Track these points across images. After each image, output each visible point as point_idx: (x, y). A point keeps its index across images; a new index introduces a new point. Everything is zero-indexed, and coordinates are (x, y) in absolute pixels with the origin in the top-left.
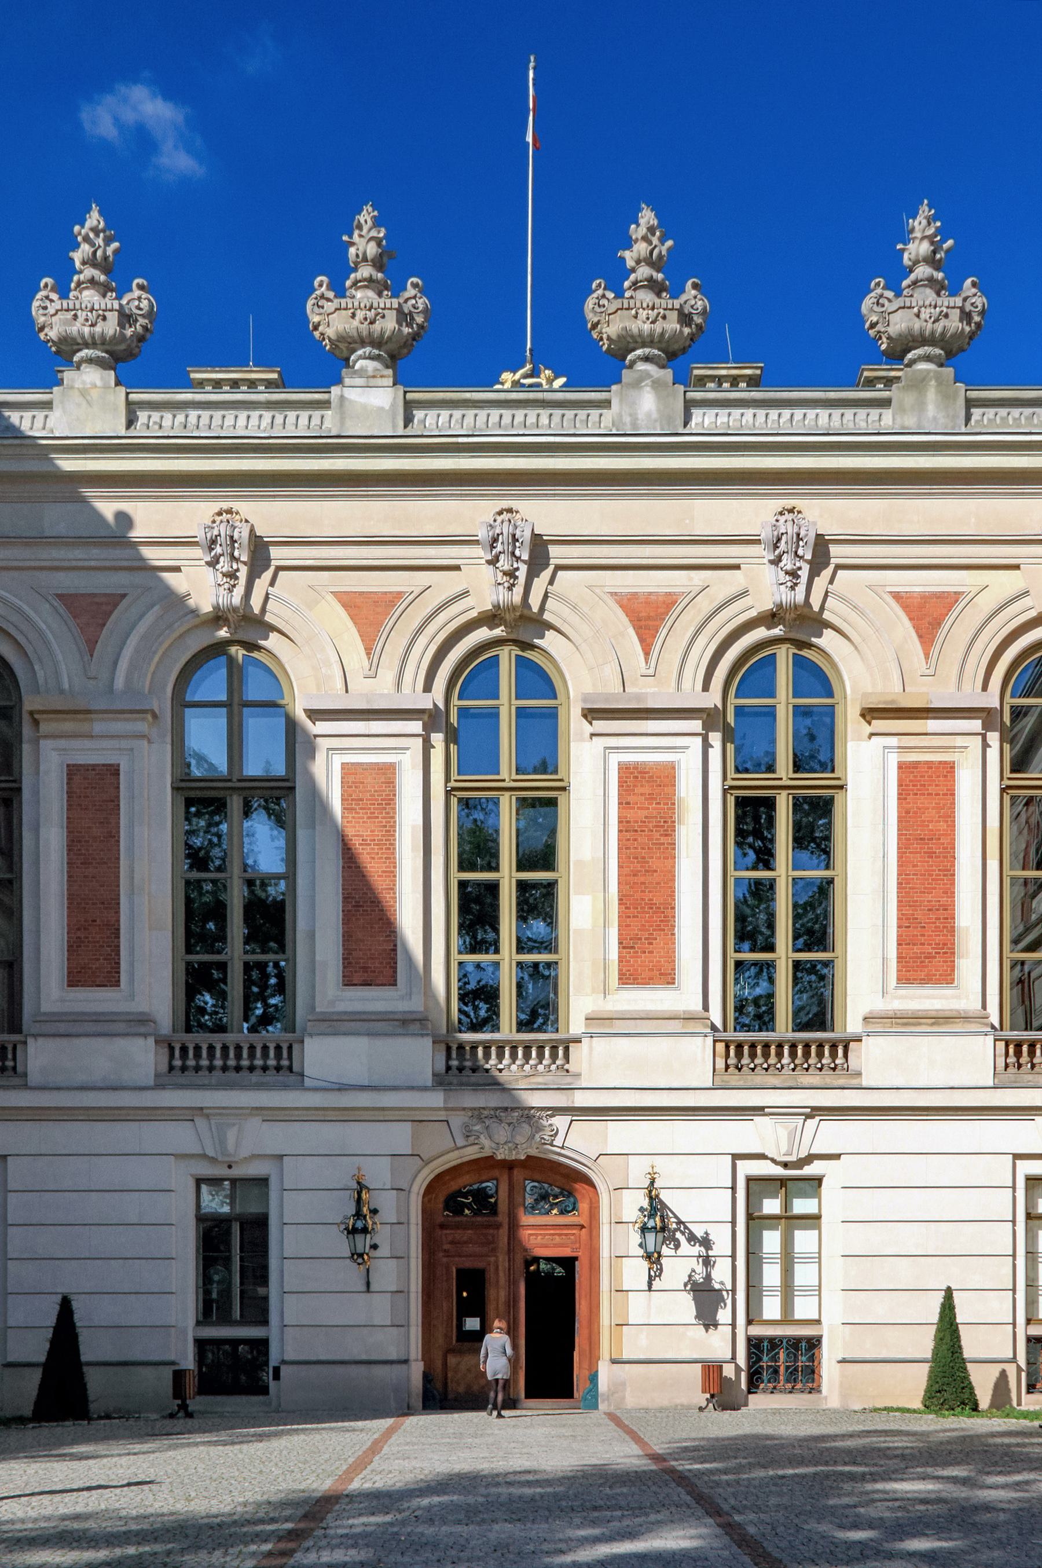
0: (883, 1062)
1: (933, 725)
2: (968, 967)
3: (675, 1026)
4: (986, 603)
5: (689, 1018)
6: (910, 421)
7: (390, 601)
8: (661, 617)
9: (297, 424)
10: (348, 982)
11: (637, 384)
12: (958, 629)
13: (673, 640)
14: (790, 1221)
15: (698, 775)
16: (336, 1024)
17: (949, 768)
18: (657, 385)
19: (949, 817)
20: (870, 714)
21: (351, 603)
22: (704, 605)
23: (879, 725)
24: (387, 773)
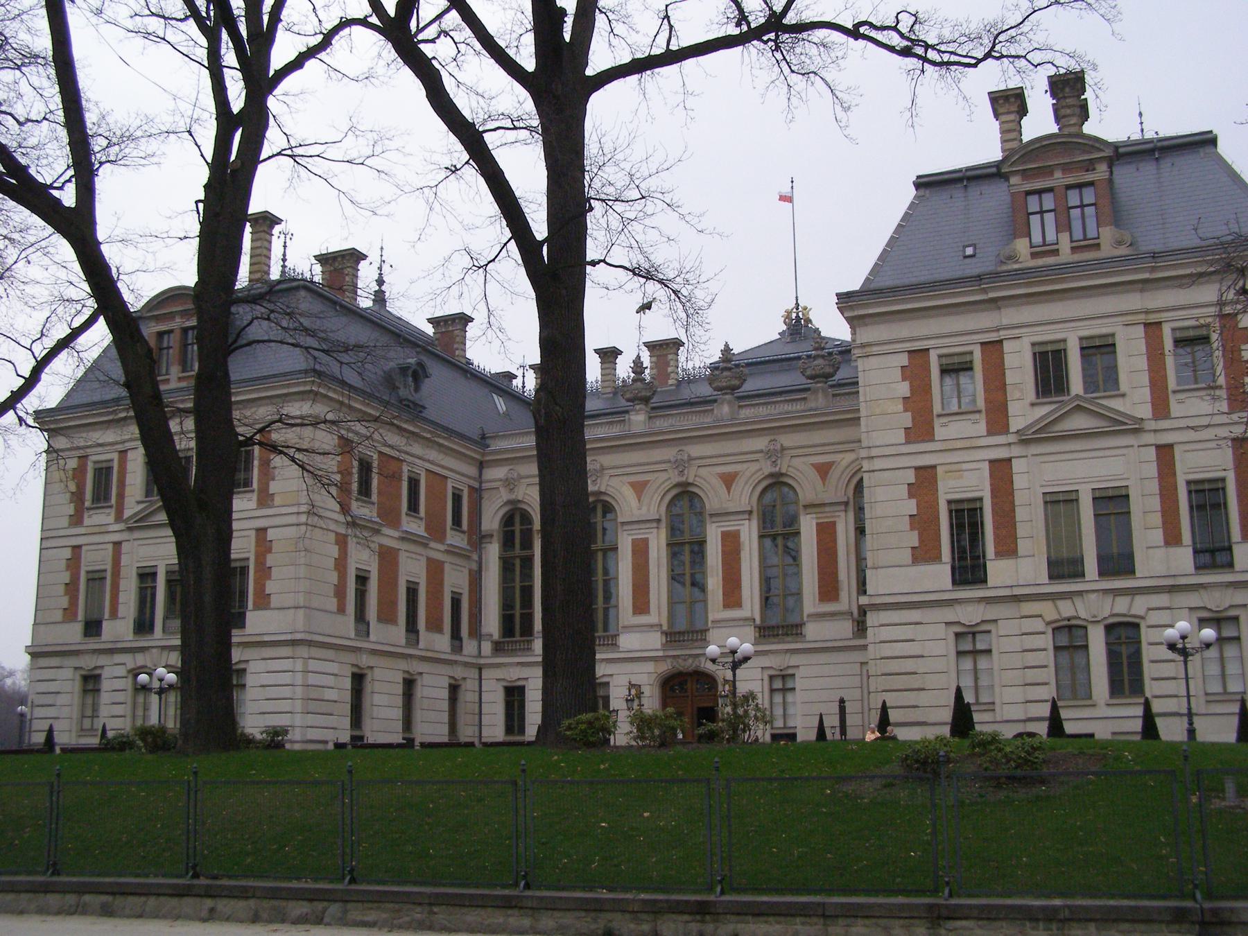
0: (813, 631)
1: (827, 509)
2: (844, 595)
3: (741, 623)
4: (844, 463)
5: (746, 619)
6: (813, 405)
7: (645, 483)
8: (733, 480)
9: (615, 430)
10: (634, 613)
11: (722, 403)
12: (834, 474)
13: (737, 486)
14: (785, 690)
15: (749, 533)
16: (630, 628)
17: (834, 524)
18: (729, 403)
19: (835, 541)
20: (805, 507)
21: (633, 485)
22: (748, 474)
23: (809, 511)
24: (646, 541)
